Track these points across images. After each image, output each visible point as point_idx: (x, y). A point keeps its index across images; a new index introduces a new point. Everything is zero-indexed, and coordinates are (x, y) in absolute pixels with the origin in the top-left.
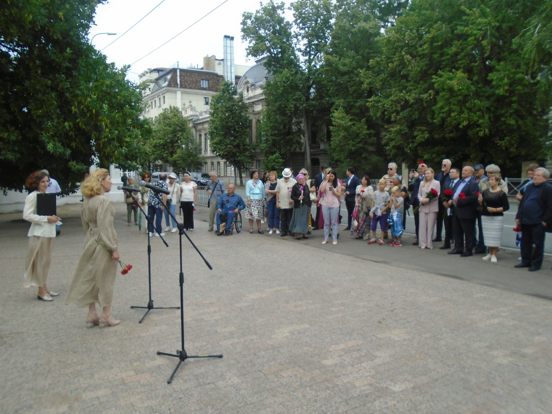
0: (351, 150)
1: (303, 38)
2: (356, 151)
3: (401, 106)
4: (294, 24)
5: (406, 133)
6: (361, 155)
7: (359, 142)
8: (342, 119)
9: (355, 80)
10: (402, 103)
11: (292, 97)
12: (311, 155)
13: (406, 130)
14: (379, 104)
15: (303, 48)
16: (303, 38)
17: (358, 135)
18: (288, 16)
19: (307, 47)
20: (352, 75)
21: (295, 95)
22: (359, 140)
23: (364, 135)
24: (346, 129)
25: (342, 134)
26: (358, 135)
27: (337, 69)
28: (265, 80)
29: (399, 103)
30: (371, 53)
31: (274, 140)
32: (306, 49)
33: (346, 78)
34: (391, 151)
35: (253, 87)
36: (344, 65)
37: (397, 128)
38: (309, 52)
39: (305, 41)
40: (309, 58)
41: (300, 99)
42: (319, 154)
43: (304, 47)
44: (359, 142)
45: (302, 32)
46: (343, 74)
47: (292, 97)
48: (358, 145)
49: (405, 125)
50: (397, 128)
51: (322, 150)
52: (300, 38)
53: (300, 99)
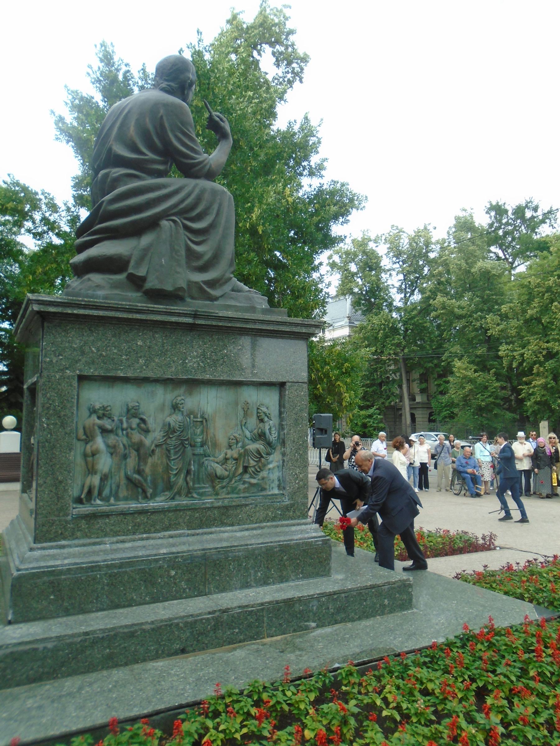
0: (480, 406)
1: (398, 273)
2: (487, 405)
3: (543, 356)
4: (384, 257)
5: (552, 387)
6: (491, 411)
7: (490, 396)
8: (465, 369)
9: (474, 325)
10: (544, 352)
11: (391, 341)
12: (411, 408)
13: (553, 383)
14: (515, 354)
15: (397, 284)
16: (398, 273)
17: (486, 388)
18: (382, 249)
19: (402, 284)
20: (471, 319)
21: (393, 339)
22: (489, 394)
23: (495, 388)
24: (471, 381)
25: (469, 387)
26: (486, 388)
27: (452, 312)
28: (347, 320)
29: (541, 353)
30: (493, 295)
31: (366, 393)
32: (401, 286)
33: (463, 322)
34: (531, 406)
35: (331, 328)
36: (460, 307)
37: (540, 382)
38: (405, 289)
39: (401, 277)
40: (405, 296)
41: (400, 343)
42: (415, 408)
43: (399, 283)
44: (490, 396)
45: (397, 266)
46: (460, 317)
47: (391, 341)
48: (487, 400)
49: (550, 378)
50: (540, 382)
51: (418, 403)
52: (394, 273)
53: (400, 343)
